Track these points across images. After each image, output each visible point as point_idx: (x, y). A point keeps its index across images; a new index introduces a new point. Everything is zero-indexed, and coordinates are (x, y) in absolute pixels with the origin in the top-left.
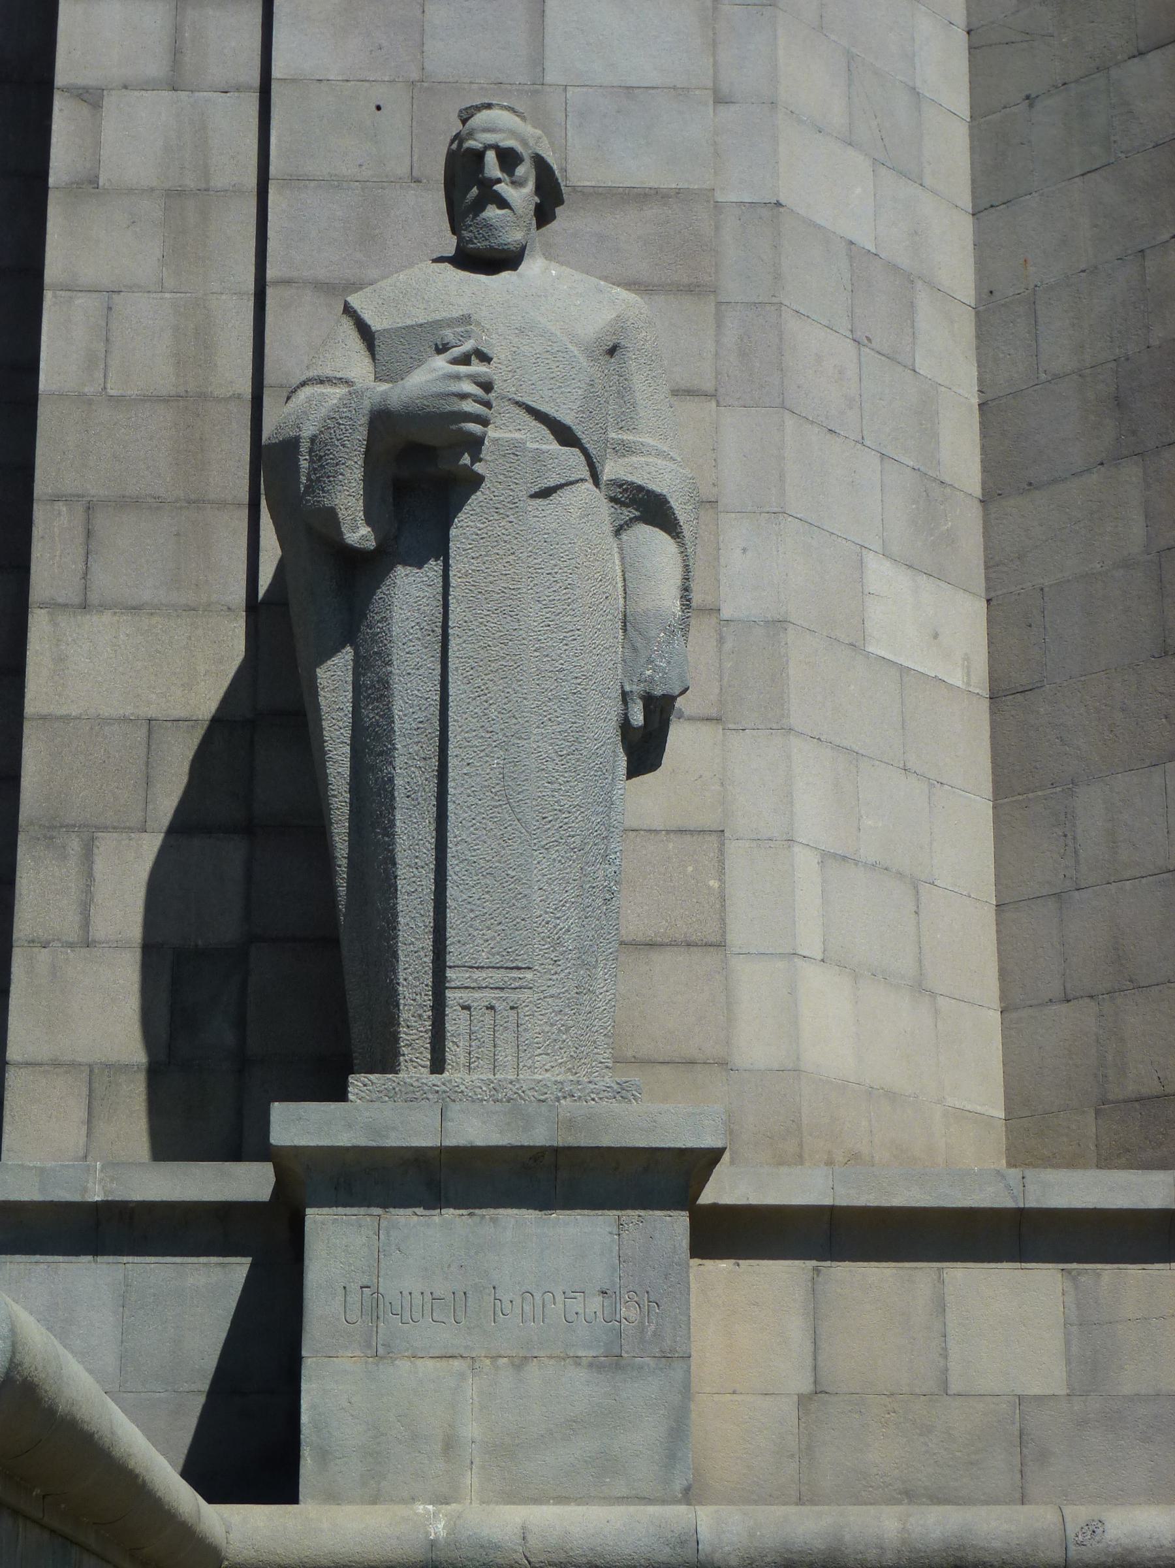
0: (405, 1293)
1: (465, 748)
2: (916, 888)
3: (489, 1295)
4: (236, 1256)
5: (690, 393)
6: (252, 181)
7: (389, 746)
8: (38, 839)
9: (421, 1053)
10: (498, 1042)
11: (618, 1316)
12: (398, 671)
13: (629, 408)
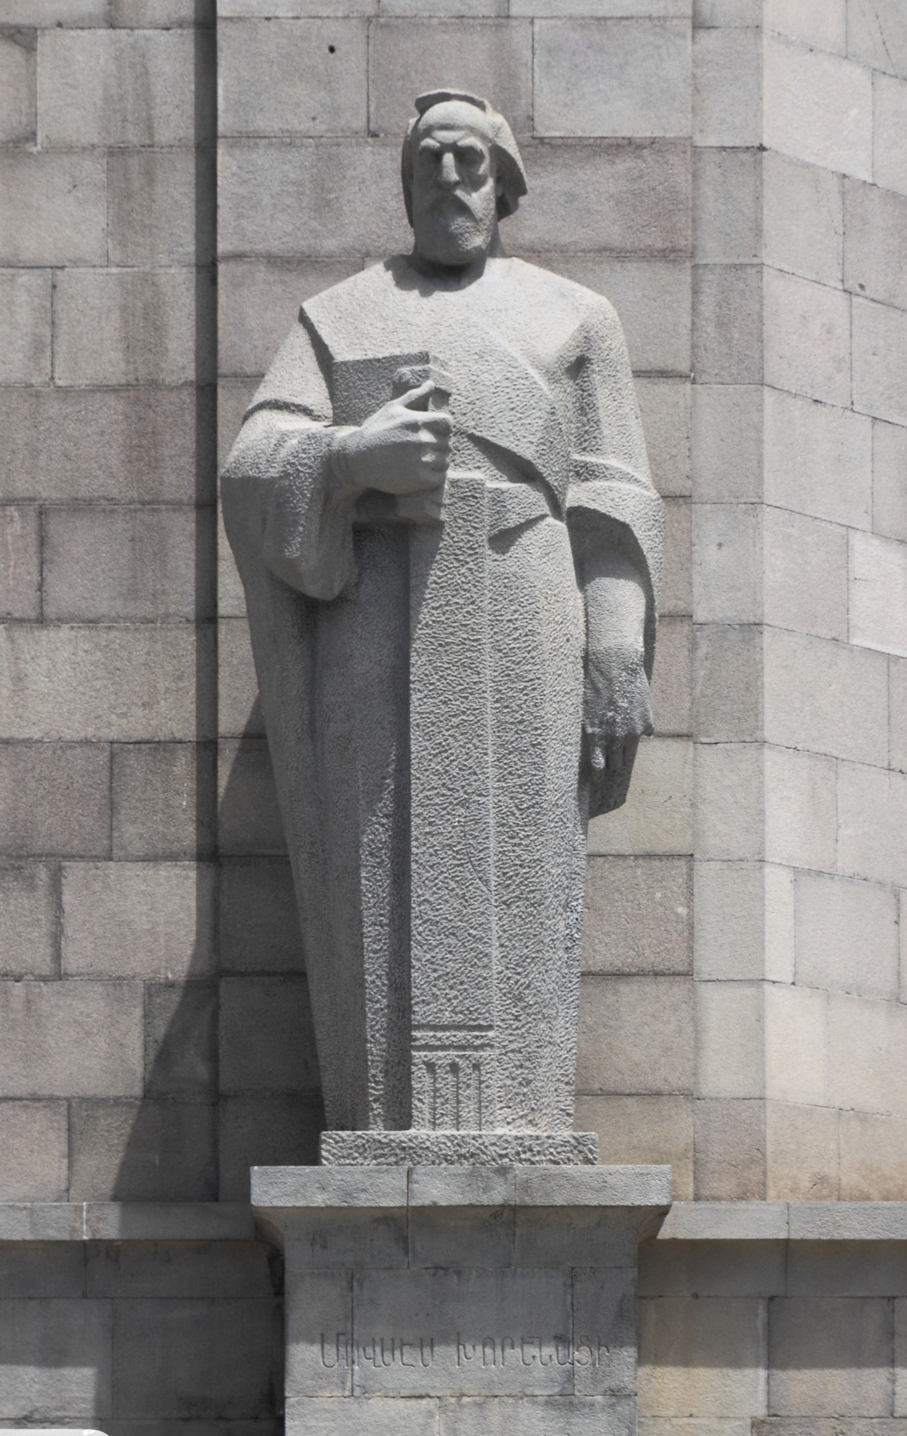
1: (427, 806)
5: (663, 374)
13: (592, 427)
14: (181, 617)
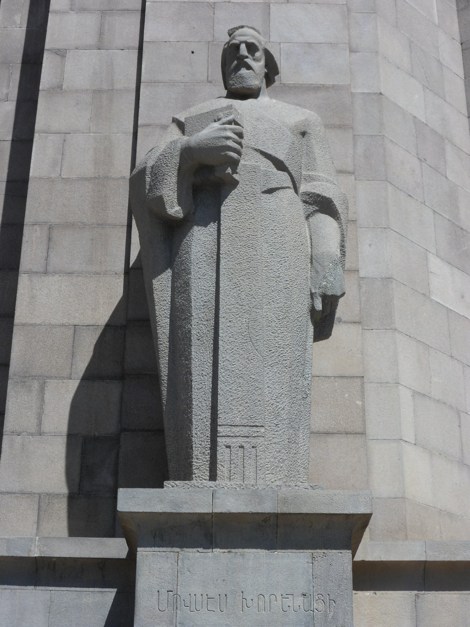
0: (192, 595)
1: (228, 313)
2: (459, 414)
3: (240, 596)
4: (109, 588)
6: (134, 86)
7: (189, 315)
8: (18, 383)
9: (204, 472)
10: (245, 465)
11: (312, 608)
12: (194, 277)
13: (312, 161)
14: (113, 272)
